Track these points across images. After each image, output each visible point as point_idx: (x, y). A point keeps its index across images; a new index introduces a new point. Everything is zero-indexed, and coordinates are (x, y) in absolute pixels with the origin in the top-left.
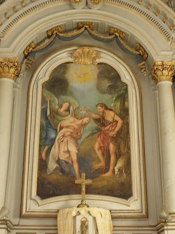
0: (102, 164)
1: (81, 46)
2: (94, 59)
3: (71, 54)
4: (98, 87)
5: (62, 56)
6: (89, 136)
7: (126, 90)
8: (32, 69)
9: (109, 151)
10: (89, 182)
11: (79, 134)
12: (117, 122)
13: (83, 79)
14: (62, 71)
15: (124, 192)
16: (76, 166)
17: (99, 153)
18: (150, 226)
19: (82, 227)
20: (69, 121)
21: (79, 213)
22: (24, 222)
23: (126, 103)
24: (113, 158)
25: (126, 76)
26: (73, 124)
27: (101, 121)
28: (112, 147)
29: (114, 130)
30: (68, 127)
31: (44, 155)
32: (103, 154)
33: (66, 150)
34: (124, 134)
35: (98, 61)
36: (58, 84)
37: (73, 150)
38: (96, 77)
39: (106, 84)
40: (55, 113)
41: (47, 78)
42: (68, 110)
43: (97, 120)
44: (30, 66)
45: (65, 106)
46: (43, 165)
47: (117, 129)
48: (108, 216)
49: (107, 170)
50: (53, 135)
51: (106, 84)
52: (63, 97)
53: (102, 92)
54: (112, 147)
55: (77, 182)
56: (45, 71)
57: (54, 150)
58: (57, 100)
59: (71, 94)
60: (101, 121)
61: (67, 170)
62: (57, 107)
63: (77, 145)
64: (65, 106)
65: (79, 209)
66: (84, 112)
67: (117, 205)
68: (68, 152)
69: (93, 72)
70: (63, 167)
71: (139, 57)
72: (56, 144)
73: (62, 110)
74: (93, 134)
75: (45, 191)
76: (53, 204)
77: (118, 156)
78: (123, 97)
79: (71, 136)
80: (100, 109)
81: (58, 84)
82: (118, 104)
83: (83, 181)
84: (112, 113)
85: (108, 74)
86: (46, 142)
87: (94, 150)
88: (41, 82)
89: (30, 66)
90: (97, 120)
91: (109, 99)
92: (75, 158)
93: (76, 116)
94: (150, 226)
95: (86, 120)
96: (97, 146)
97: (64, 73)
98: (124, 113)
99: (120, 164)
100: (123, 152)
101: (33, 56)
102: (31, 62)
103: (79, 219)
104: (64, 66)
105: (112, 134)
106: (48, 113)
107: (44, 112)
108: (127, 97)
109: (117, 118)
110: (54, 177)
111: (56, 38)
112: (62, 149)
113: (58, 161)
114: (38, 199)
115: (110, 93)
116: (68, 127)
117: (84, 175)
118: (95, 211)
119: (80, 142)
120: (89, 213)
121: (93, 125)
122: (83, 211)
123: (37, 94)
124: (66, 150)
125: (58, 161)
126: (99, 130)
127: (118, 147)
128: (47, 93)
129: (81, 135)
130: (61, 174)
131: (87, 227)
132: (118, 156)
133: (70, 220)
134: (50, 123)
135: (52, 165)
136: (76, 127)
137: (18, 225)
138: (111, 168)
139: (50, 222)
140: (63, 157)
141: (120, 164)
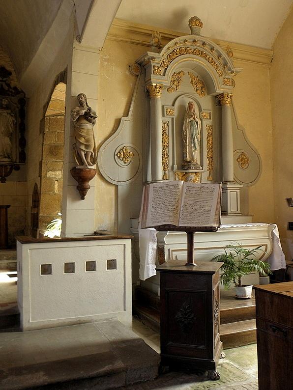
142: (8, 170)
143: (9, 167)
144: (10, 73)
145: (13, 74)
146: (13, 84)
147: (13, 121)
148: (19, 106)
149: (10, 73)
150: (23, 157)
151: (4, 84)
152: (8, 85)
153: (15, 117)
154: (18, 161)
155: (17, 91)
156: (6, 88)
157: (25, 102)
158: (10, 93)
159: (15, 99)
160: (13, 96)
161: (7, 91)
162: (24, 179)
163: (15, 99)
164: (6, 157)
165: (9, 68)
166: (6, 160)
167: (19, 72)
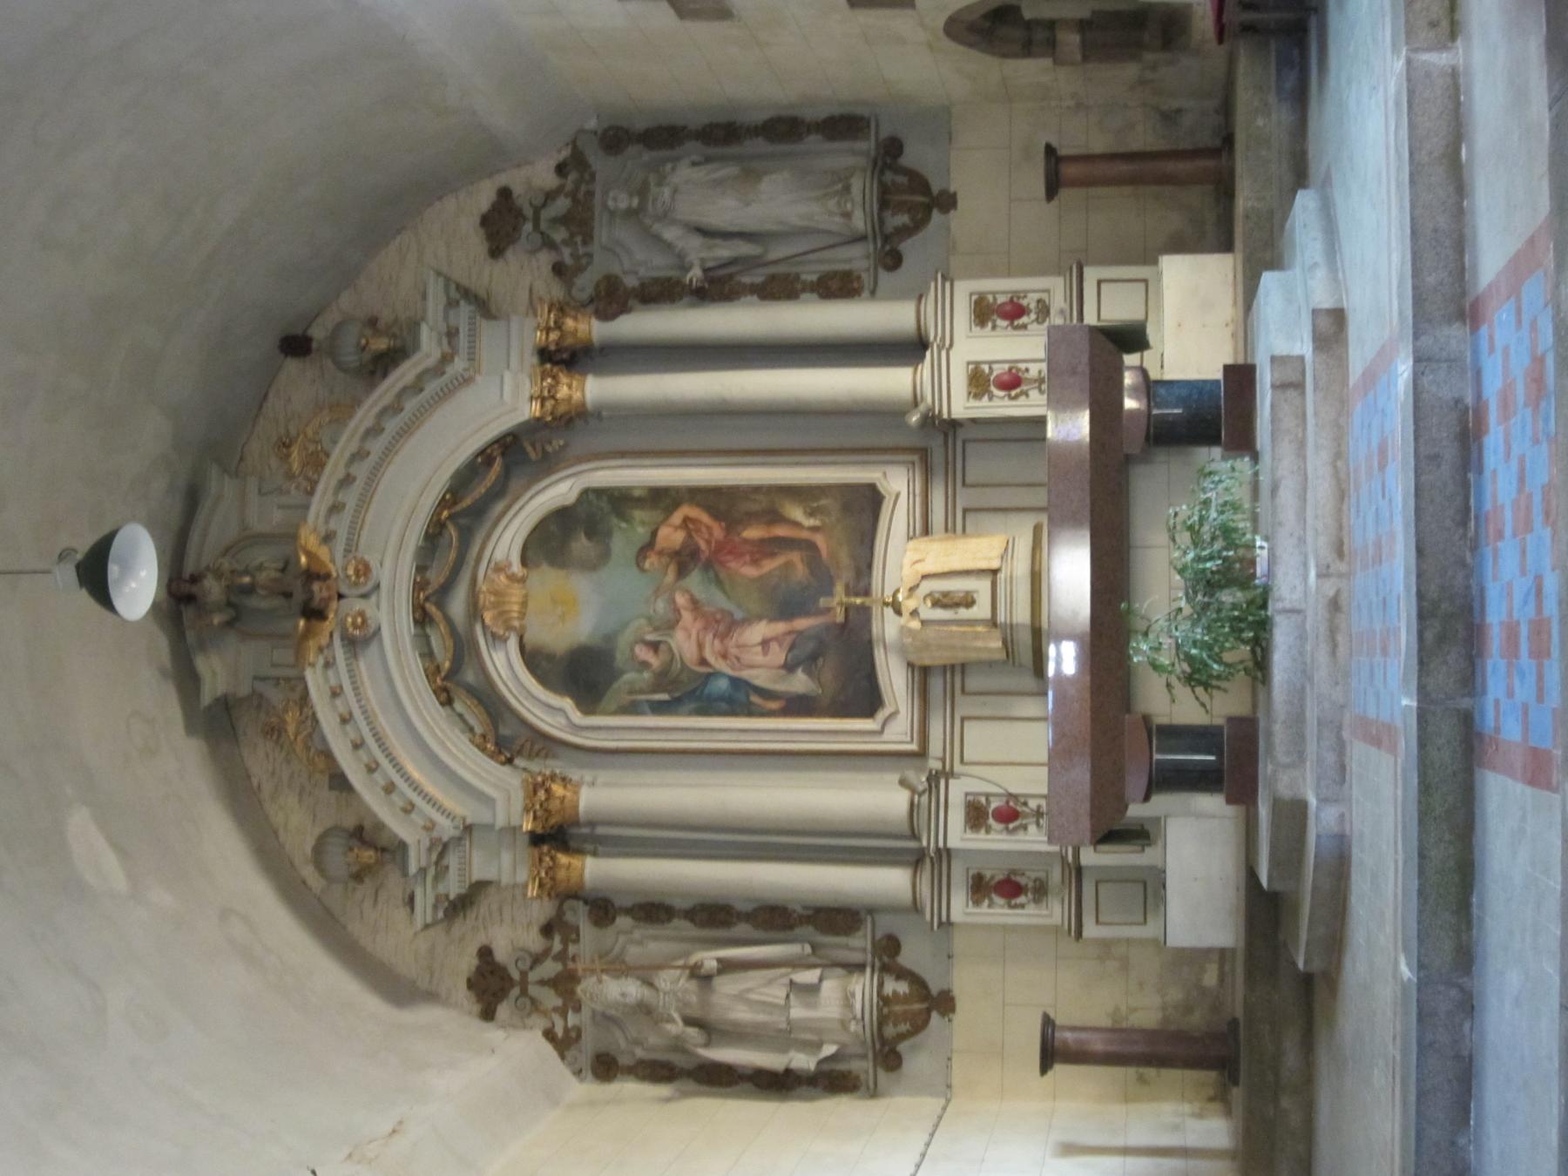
0: (795, 557)
1: (475, 612)
2: (512, 578)
3: (497, 639)
4: (591, 566)
5: (503, 665)
6: (725, 592)
7: (599, 492)
8: (544, 745)
9: (762, 541)
10: (839, 589)
11: (718, 616)
12: (686, 520)
13: (572, 608)
14: (544, 663)
15: (868, 502)
16: (802, 623)
17: (769, 565)
18: (946, 443)
19: (945, 606)
20: (684, 643)
21: (914, 613)
22: (935, 747)
23: (637, 493)
24: (781, 531)
25: (560, 491)
26: (694, 636)
27: (684, 559)
28: (753, 533)
29: (708, 528)
30: (700, 646)
31: (774, 705)
32: (772, 555)
33: (759, 651)
34: (715, 499)
35: (516, 568)
36: (583, 674)
37: (759, 631)
38: (562, 573)
39: (581, 545)
40: (664, 679)
41: (567, 703)
42: (655, 646)
43: (682, 572)
44: (537, 747)
45: (643, 653)
46: (799, 706)
47: (705, 518)
48: (922, 544)
49: (810, 546)
50: (722, 685)
51: (581, 545)
52: (620, 658)
53: (605, 556)
54: (753, 533)
55: (840, 618)
56: (549, 710)
57: (760, 678)
58: (628, 676)
59: (610, 638)
60: (684, 559)
61: (810, 646)
62: (646, 675)
63: (747, 621)
64: (643, 653)
65: (906, 613)
66: (661, 606)
67: (897, 519)
68: (765, 643)
69: (547, 580)
70: (803, 656)
71: (515, 456)
72: (745, 674)
73: (655, 661)
74: (719, 582)
75: (863, 697)
76: (894, 679)
77: (774, 517)
78: (620, 500)
79: (724, 636)
80: (651, 562)
81: (583, 674)
82: (638, 514)
83: (838, 600)
84: (664, 532)
85: (552, 540)
86: (741, 699)
87: (761, 577)
88: (577, 717)
89: (537, 747)
90: (682, 572)
91: (625, 537)
92: (780, 627)
93: (671, 625)
94: (946, 443)
95: (681, 600)
96: (750, 571)
97: (550, 657)
98: (662, 499)
99: (796, 513)
100: (767, 503)
101: (507, 738)
102: (528, 745)
103: (928, 612)
104: (534, 659)
105: (718, 532)
106: (664, 697)
107: (659, 708)
108: (619, 489)
109: (677, 518)
110: (828, 676)
111: (459, 680)
112: (760, 659)
113: (789, 667)
114: (881, 715)
115: (608, 534)
116: (700, 646)
117: (823, 602)
118: (909, 574)
119: (739, 615)
120: (912, 590)
121: (695, 581)
122: (909, 605)
123: (609, 728)
124: (759, 651)
125: (789, 667)
126: (708, 566)
127: (752, 518)
128: (610, 700)
129: (722, 611)
130: (821, 660)
131: (946, 594)
132: (774, 517)
133: (931, 632)
134: (689, 691)
135: (800, 683)
136: (699, 625)
137: (943, 760)
138: (805, 535)
139: (936, 685)
140: (778, 655)
141: (796, 513)
142: (902, 179)
143: (889, 177)
144: (505, 194)
145: (502, 180)
146: (549, 180)
147: (694, 164)
148: (632, 150)
149: (505, 194)
150: (844, 125)
151: (546, 214)
152: (550, 196)
153: (677, 159)
154: (861, 145)
155: (573, 165)
156: (562, 205)
157: (610, 128)
158: (583, 188)
159: (601, 164)
160: (593, 176)
161: (575, 200)
162: (939, 121)
163: (601, 164)
164: (847, 189)
165: (484, 197)
166: (857, 184)
167: (491, 153)
